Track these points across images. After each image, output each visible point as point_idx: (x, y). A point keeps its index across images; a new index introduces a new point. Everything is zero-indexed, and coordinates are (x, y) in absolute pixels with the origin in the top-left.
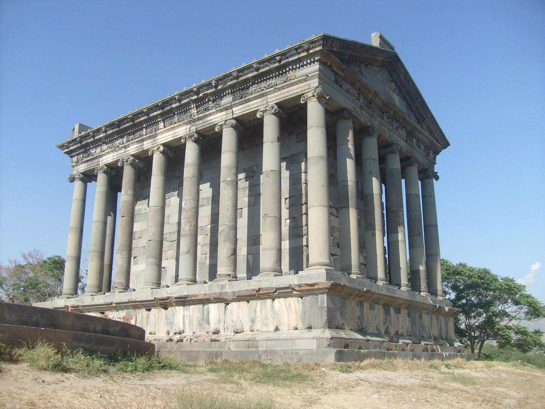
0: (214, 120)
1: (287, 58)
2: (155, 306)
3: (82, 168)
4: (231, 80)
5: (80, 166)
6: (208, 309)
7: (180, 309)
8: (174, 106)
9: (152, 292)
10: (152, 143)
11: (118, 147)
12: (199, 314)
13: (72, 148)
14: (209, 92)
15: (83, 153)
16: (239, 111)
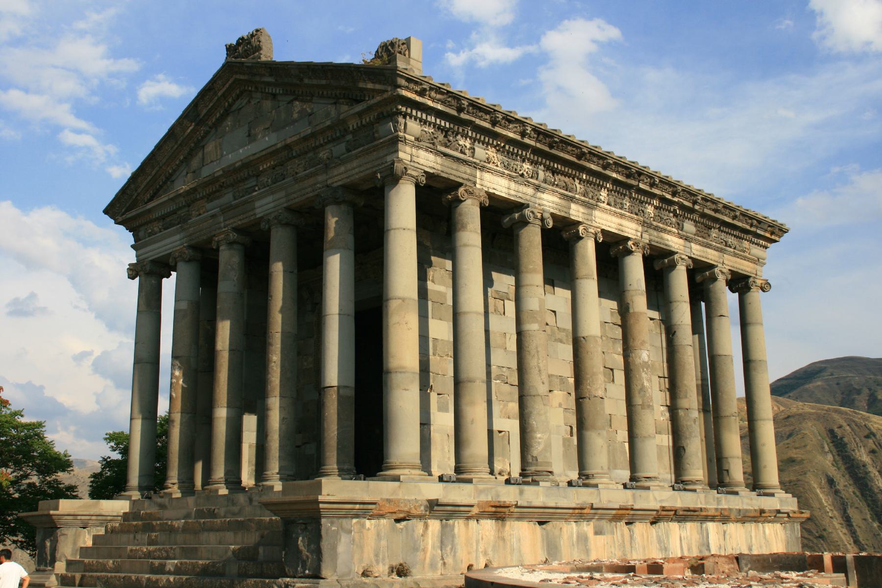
0: (670, 243)
1: (757, 227)
2: (642, 519)
3: (427, 161)
4: (710, 209)
5: (422, 153)
6: (707, 530)
7: (674, 526)
8: (642, 186)
9: (634, 496)
10: (586, 217)
11: (522, 175)
12: (698, 536)
13: (430, 103)
14: (686, 203)
15: (439, 128)
16: (697, 251)
